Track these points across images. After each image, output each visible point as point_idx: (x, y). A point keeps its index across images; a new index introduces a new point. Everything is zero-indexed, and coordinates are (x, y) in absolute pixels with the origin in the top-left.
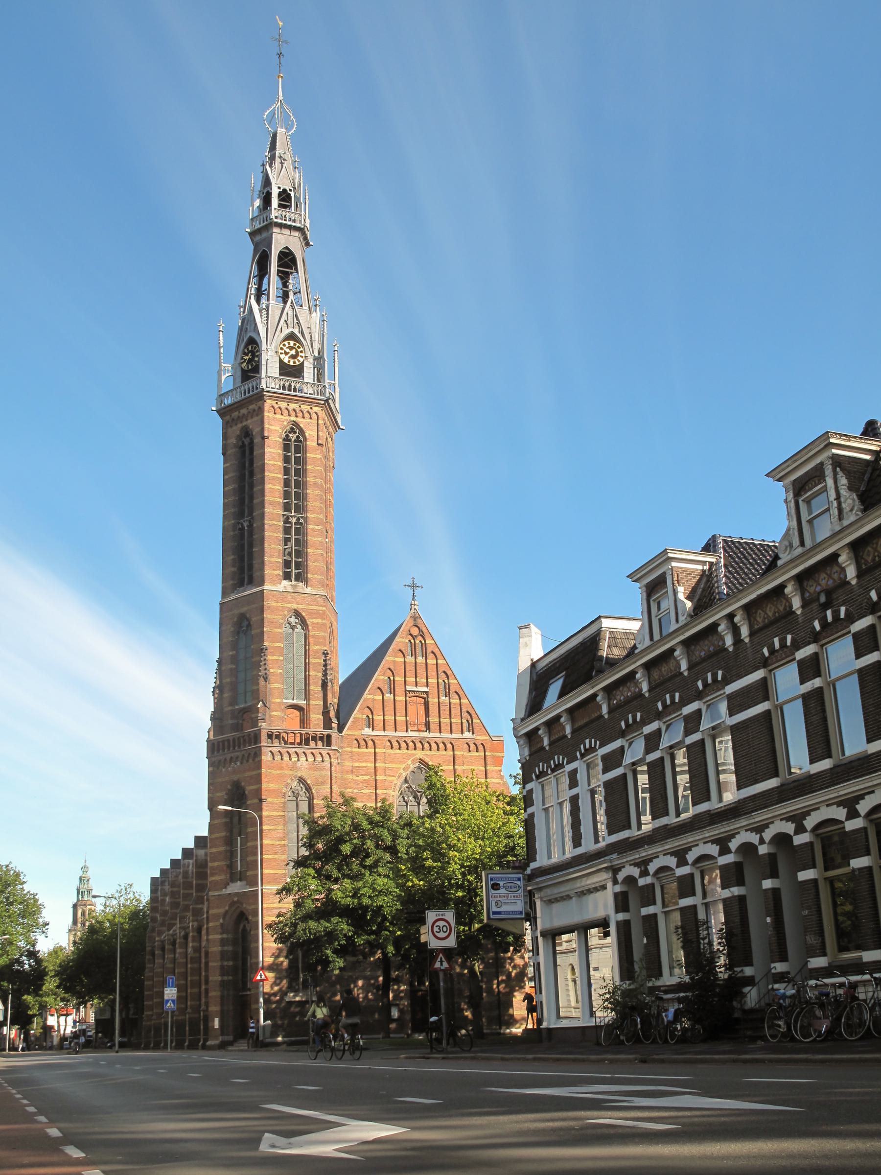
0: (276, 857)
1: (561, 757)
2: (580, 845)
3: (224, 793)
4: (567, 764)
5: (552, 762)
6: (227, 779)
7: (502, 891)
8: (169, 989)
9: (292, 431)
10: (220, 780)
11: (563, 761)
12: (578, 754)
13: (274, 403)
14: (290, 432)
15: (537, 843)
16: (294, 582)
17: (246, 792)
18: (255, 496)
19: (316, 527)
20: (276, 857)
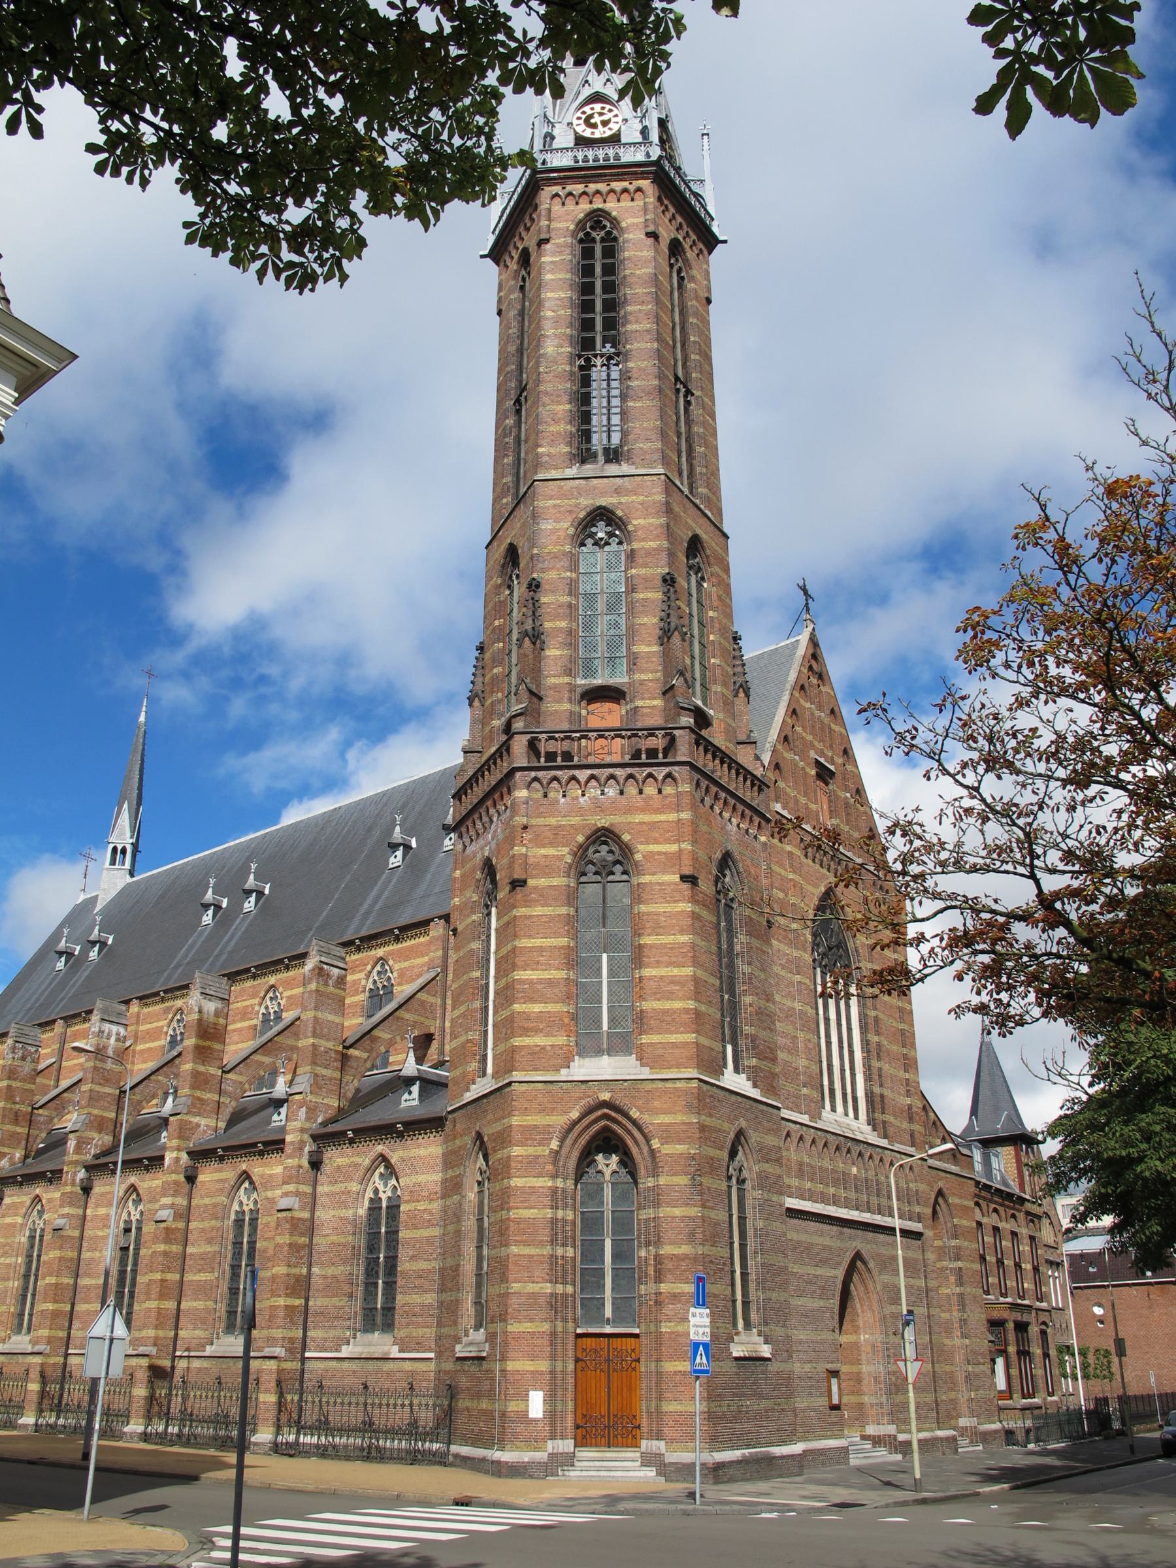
3: (566, 850)
6: (575, 820)
10: (552, 821)
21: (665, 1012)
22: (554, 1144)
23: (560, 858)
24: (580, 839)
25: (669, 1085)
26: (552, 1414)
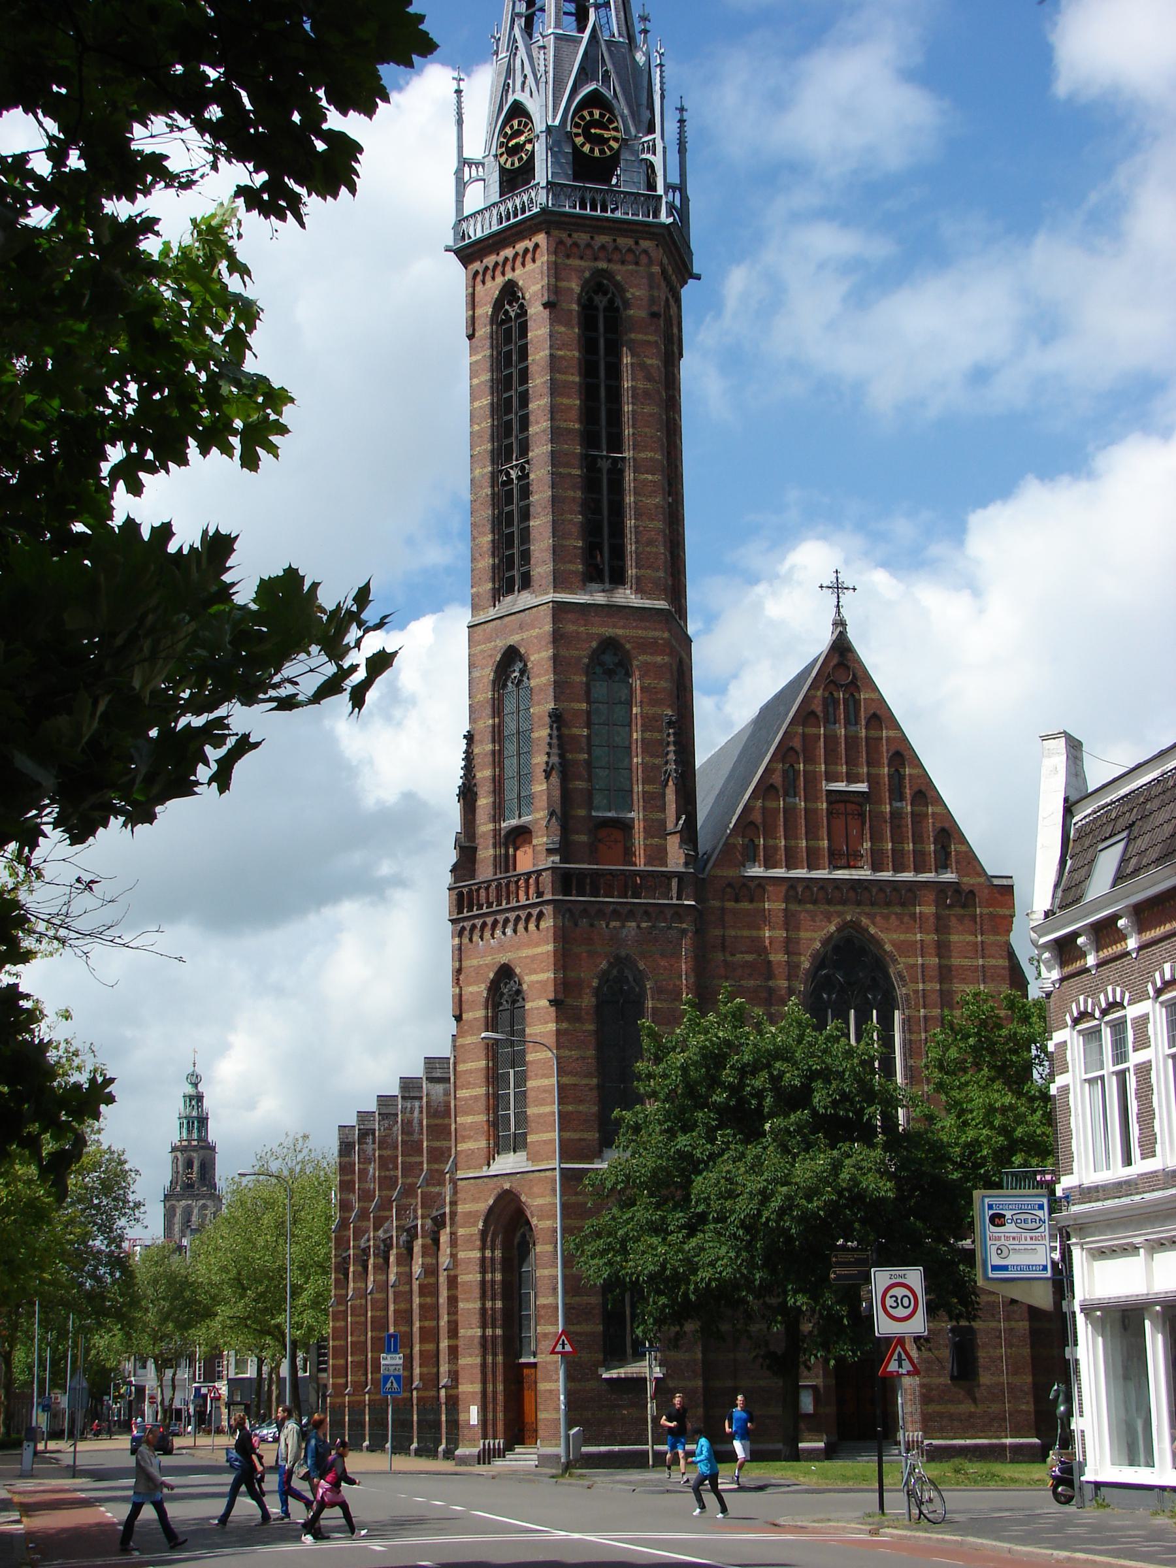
0: (582, 1108)
1: (1118, 989)
2: (1153, 1154)
3: (483, 987)
4: (1129, 1004)
5: (1102, 997)
7: (1010, 1227)
8: (389, 1356)
9: (600, 289)
11: (1122, 998)
12: (1150, 988)
13: (564, 236)
14: (596, 292)
15: (1074, 1142)
16: (607, 586)
17: (525, 987)
18: (532, 418)
19: (650, 477)
20: (582, 1108)
21: (540, 1116)
22: (480, 1225)
23: (480, 993)
24: (491, 975)
25: (542, 1174)
26: (484, 1422)
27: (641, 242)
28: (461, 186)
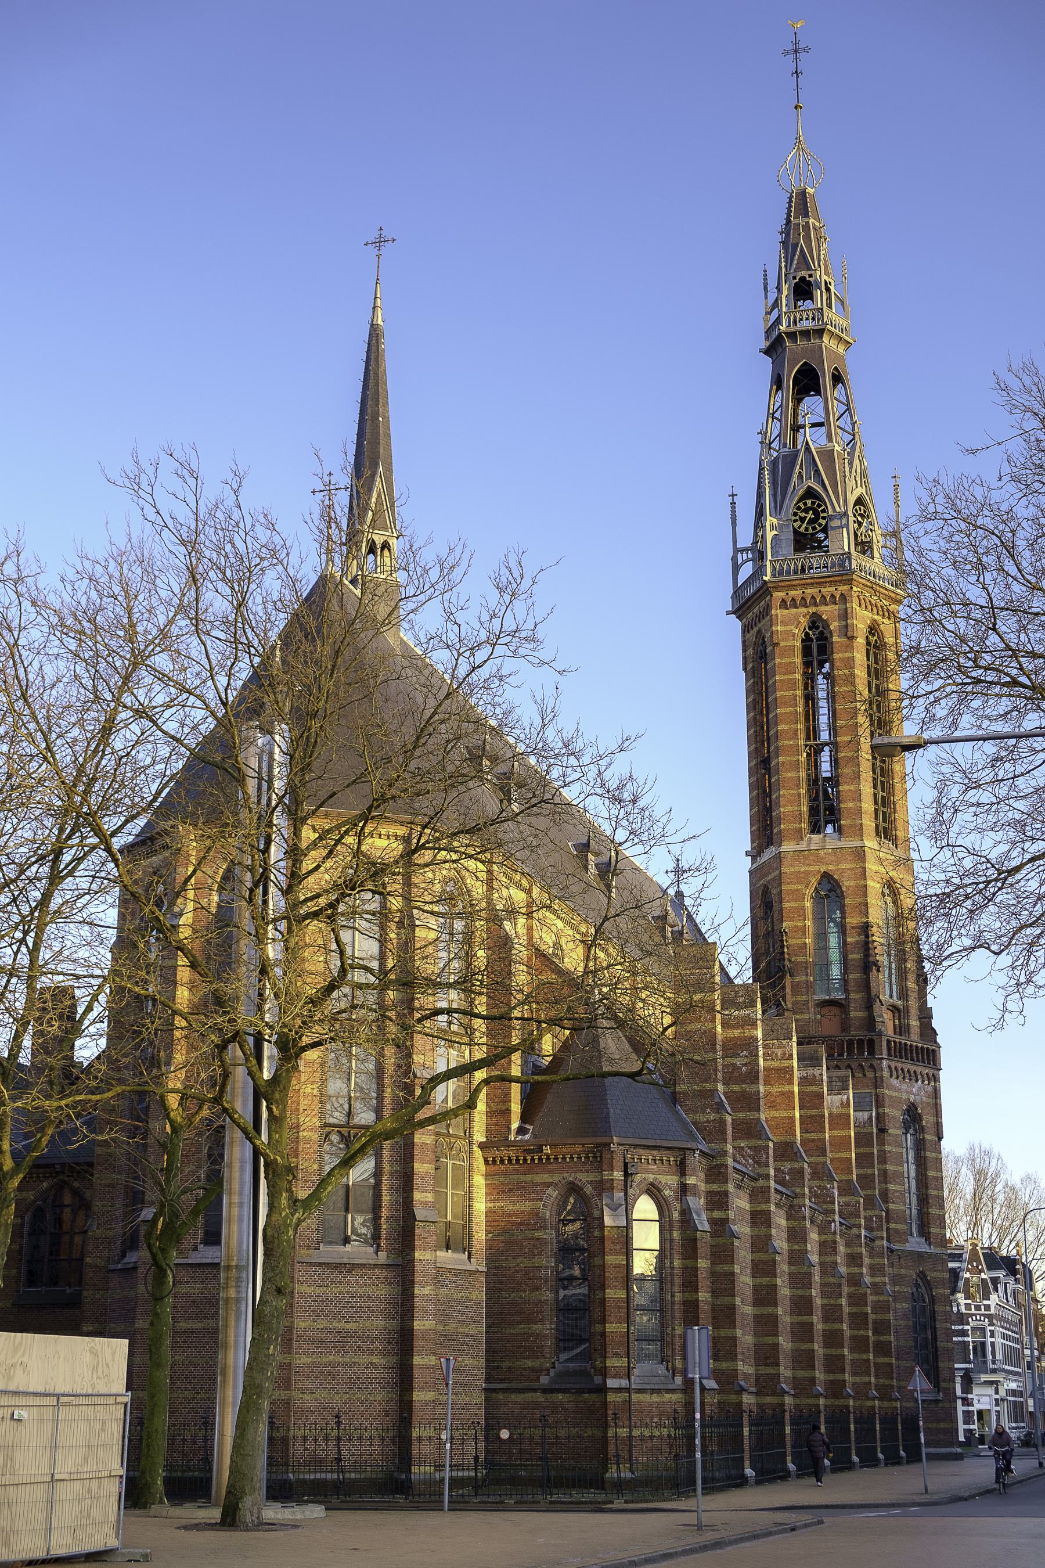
27: (839, 588)
28: (736, 568)
